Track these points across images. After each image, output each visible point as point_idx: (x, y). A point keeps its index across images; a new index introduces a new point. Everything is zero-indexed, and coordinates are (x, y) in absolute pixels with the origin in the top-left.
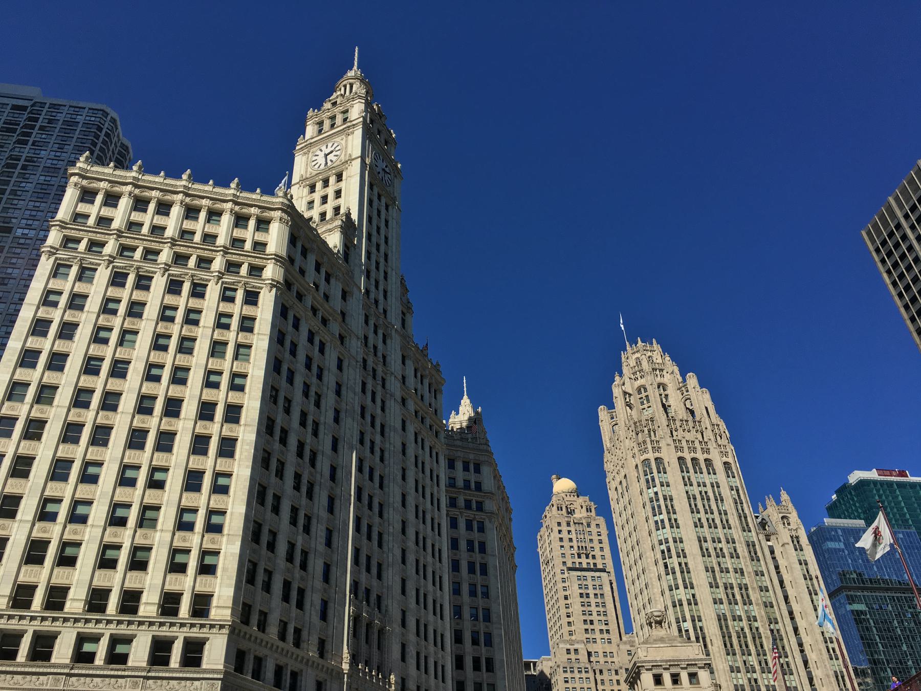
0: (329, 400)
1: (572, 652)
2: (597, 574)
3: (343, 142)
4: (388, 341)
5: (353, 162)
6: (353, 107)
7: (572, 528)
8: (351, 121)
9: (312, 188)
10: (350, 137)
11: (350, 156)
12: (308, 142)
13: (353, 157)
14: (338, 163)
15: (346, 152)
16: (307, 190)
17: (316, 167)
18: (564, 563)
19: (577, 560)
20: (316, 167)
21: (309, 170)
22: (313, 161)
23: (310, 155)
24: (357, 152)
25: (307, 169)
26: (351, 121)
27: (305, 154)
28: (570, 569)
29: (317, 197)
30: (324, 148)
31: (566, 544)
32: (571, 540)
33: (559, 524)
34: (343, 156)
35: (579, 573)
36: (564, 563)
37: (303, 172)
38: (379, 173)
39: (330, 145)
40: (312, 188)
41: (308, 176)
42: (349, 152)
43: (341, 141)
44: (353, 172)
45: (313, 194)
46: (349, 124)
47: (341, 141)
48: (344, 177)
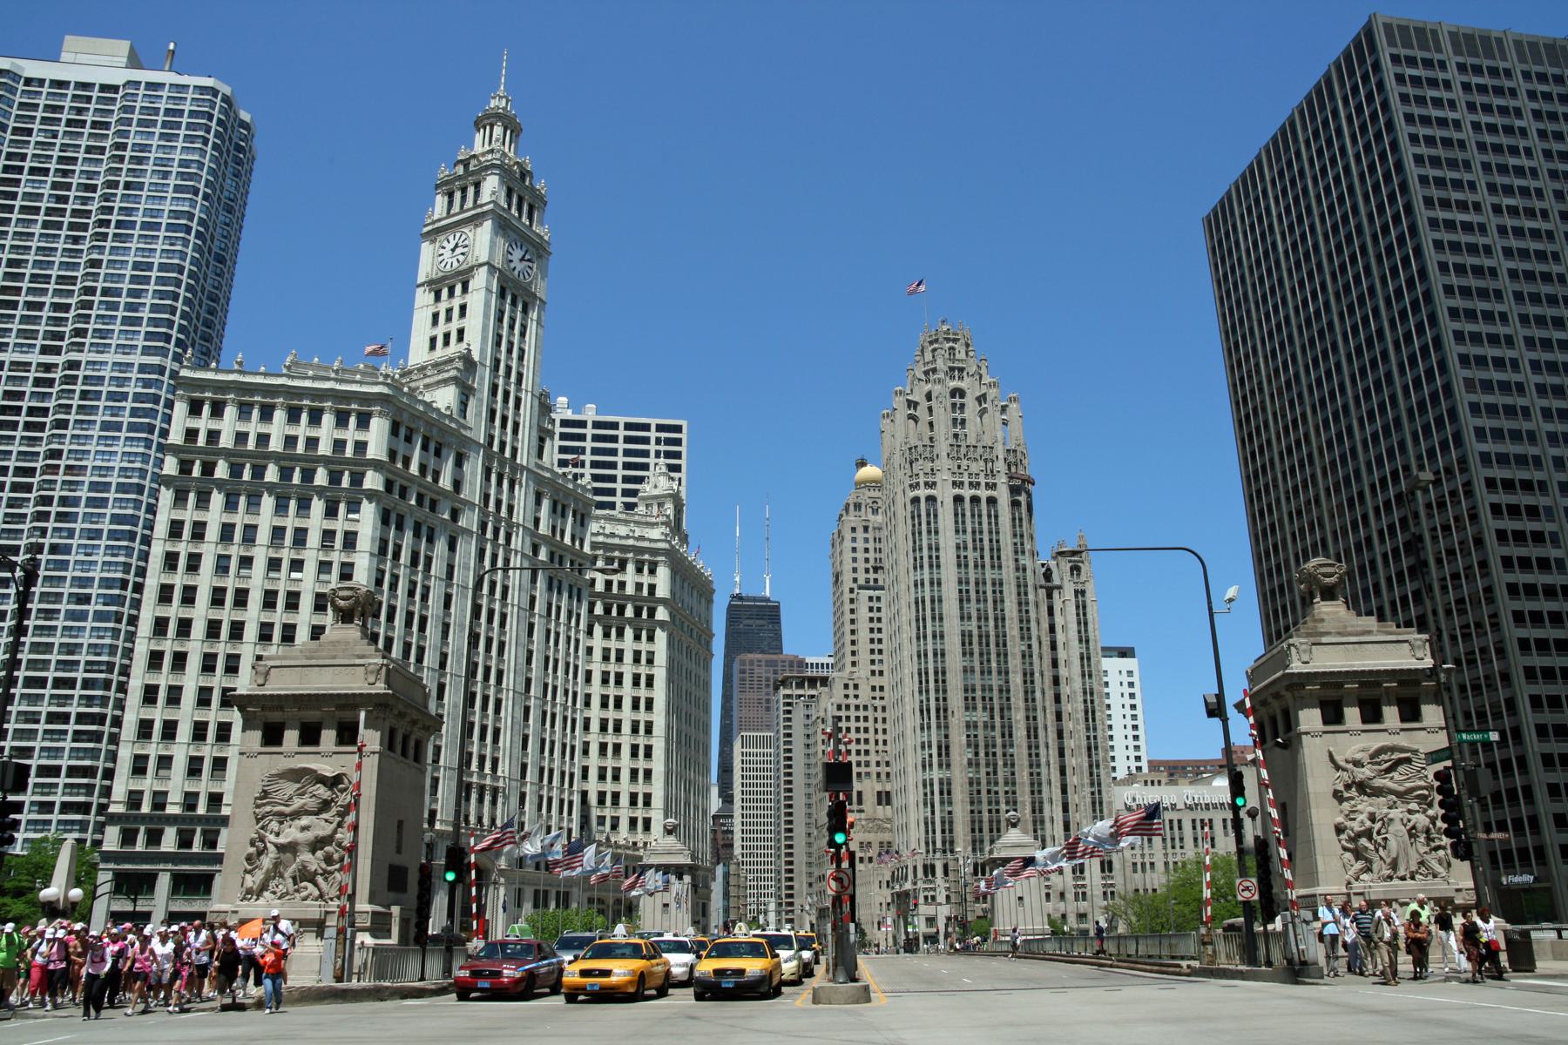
1: (851, 687)
7: (870, 535)
9: (438, 298)
10: (479, 230)
12: (436, 226)
14: (464, 267)
18: (855, 580)
19: (872, 576)
26: (482, 206)
28: (860, 588)
29: (442, 308)
30: (451, 238)
35: (871, 593)
36: (855, 580)
37: (429, 270)
39: (458, 235)
40: (438, 298)
42: (476, 253)
44: (480, 280)
46: (479, 210)
48: (470, 290)
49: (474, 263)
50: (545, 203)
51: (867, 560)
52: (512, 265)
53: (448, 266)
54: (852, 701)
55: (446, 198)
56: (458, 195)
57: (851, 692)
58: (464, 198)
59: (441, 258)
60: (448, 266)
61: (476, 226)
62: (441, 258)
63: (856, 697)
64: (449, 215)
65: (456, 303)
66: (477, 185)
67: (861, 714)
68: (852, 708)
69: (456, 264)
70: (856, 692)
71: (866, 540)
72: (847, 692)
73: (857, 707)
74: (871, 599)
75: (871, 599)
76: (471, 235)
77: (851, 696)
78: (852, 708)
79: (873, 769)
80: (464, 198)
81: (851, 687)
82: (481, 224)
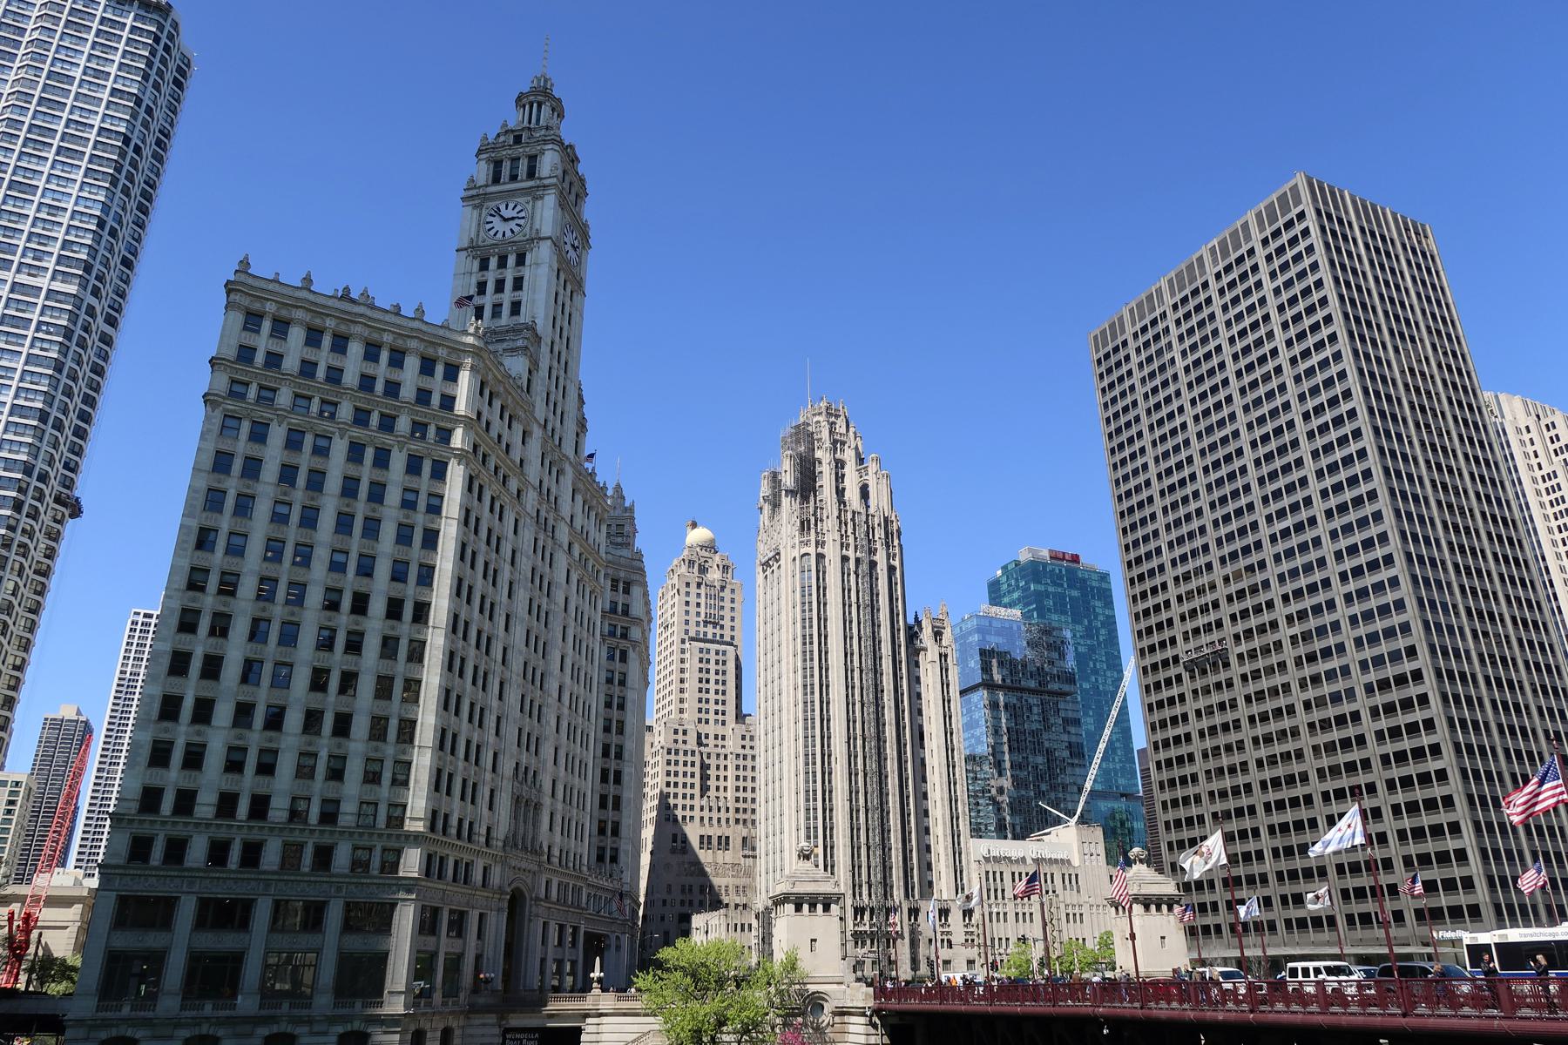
0: (506, 574)
1: (680, 732)
2: (723, 647)
3: (529, 207)
4: (561, 478)
7: (703, 591)
9: (484, 266)
10: (539, 203)
16: (476, 264)
17: (492, 233)
18: (687, 632)
19: (702, 629)
20: (492, 233)
21: (482, 233)
27: (475, 207)
28: (692, 639)
29: (491, 278)
31: (693, 609)
32: (698, 605)
33: (688, 584)
34: (528, 229)
35: (702, 645)
36: (687, 632)
40: (484, 266)
45: (485, 273)
51: (698, 614)
53: (500, 235)
54: (681, 746)
57: (680, 737)
60: (500, 235)
61: (535, 199)
63: (685, 742)
67: (689, 759)
68: (681, 753)
69: (508, 234)
70: (685, 738)
71: (699, 595)
72: (676, 737)
73: (685, 753)
74: (701, 651)
75: (701, 651)
77: (680, 741)
78: (681, 753)
79: (697, 813)
81: (680, 732)
82: (542, 198)
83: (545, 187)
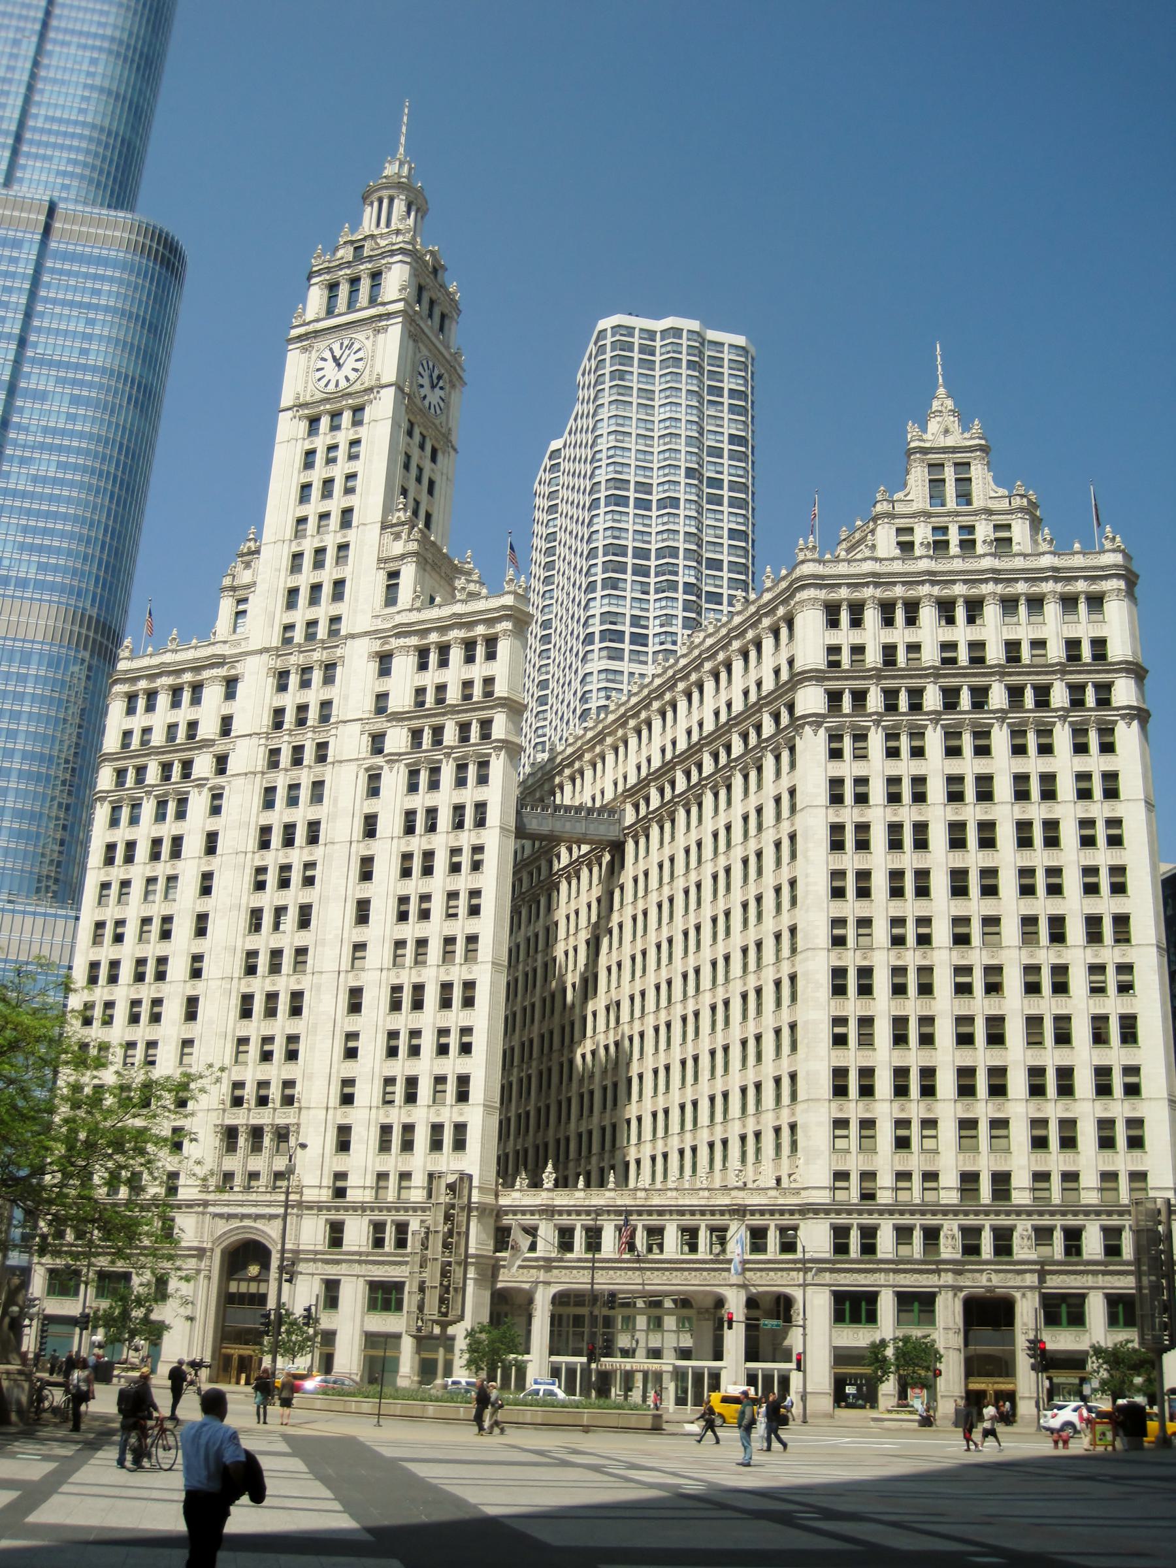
3: (369, 344)
5: (383, 391)
6: (390, 269)
8: (384, 304)
10: (381, 336)
11: (378, 379)
13: (384, 381)
14: (357, 387)
15: (372, 367)
16: (304, 425)
17: (324, 381)
20: (324, 381)
22: (318, 370)
23: (314, 355)
24: (390, 374)
25: (306, 382)
26: (384, 304)
37: (300, 389)
38: (425, 397)
41: (308, 399)
42: (377, 369)
43: (366, 342)
44: (383, 408)
46: (380, 310)
47: (366, 342)
49: (373, 383)
50: (459, 312)
52: (423, 392)
55: (326, 293)
56: (344, 290)
58: (354, 292)
59: (319, 374)
60: (331, 387)
61: (377, 331)
62: (319, 374)
64: (330, 312)
65: (342, 438)
66: (376, 276)
69: (343, 384)
76: (369, 344)
80: (354, 292)
83: (389, 316)
